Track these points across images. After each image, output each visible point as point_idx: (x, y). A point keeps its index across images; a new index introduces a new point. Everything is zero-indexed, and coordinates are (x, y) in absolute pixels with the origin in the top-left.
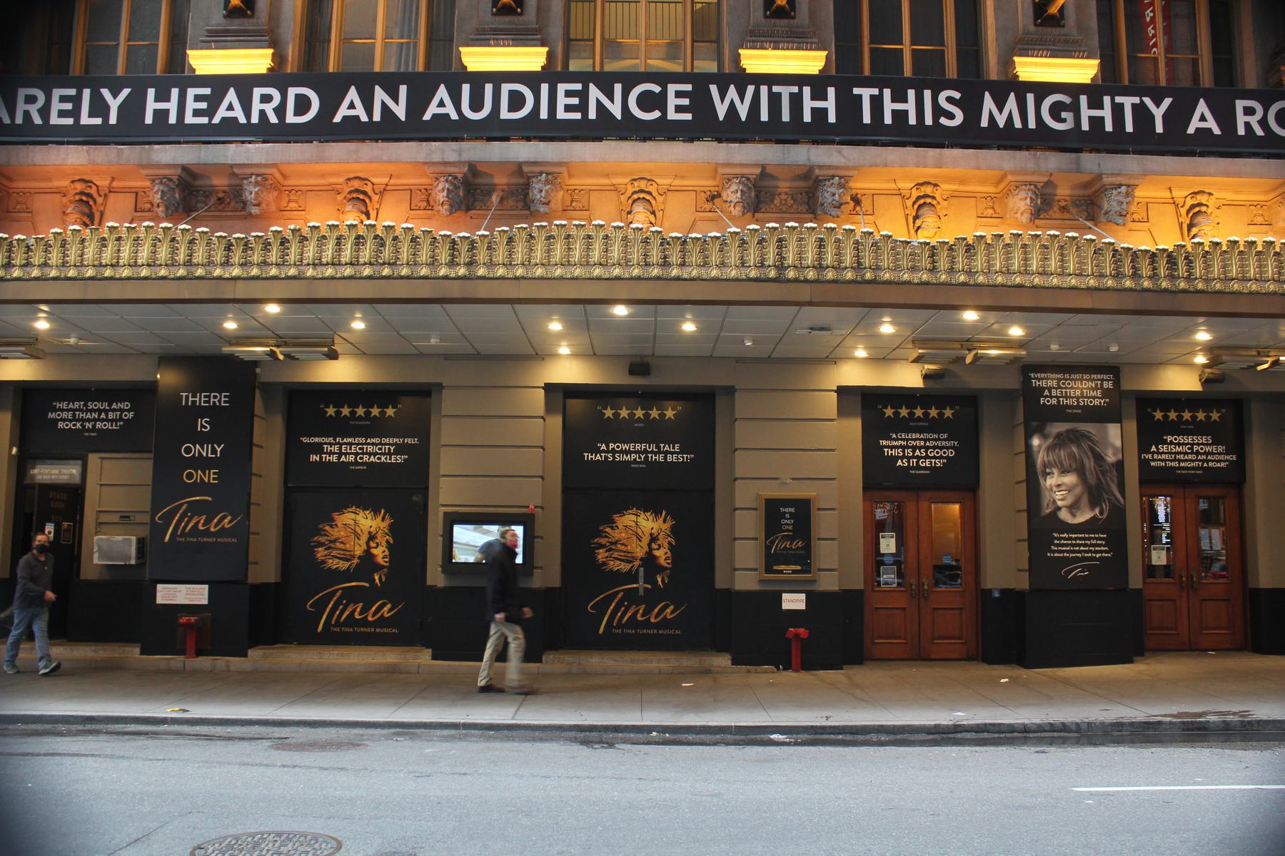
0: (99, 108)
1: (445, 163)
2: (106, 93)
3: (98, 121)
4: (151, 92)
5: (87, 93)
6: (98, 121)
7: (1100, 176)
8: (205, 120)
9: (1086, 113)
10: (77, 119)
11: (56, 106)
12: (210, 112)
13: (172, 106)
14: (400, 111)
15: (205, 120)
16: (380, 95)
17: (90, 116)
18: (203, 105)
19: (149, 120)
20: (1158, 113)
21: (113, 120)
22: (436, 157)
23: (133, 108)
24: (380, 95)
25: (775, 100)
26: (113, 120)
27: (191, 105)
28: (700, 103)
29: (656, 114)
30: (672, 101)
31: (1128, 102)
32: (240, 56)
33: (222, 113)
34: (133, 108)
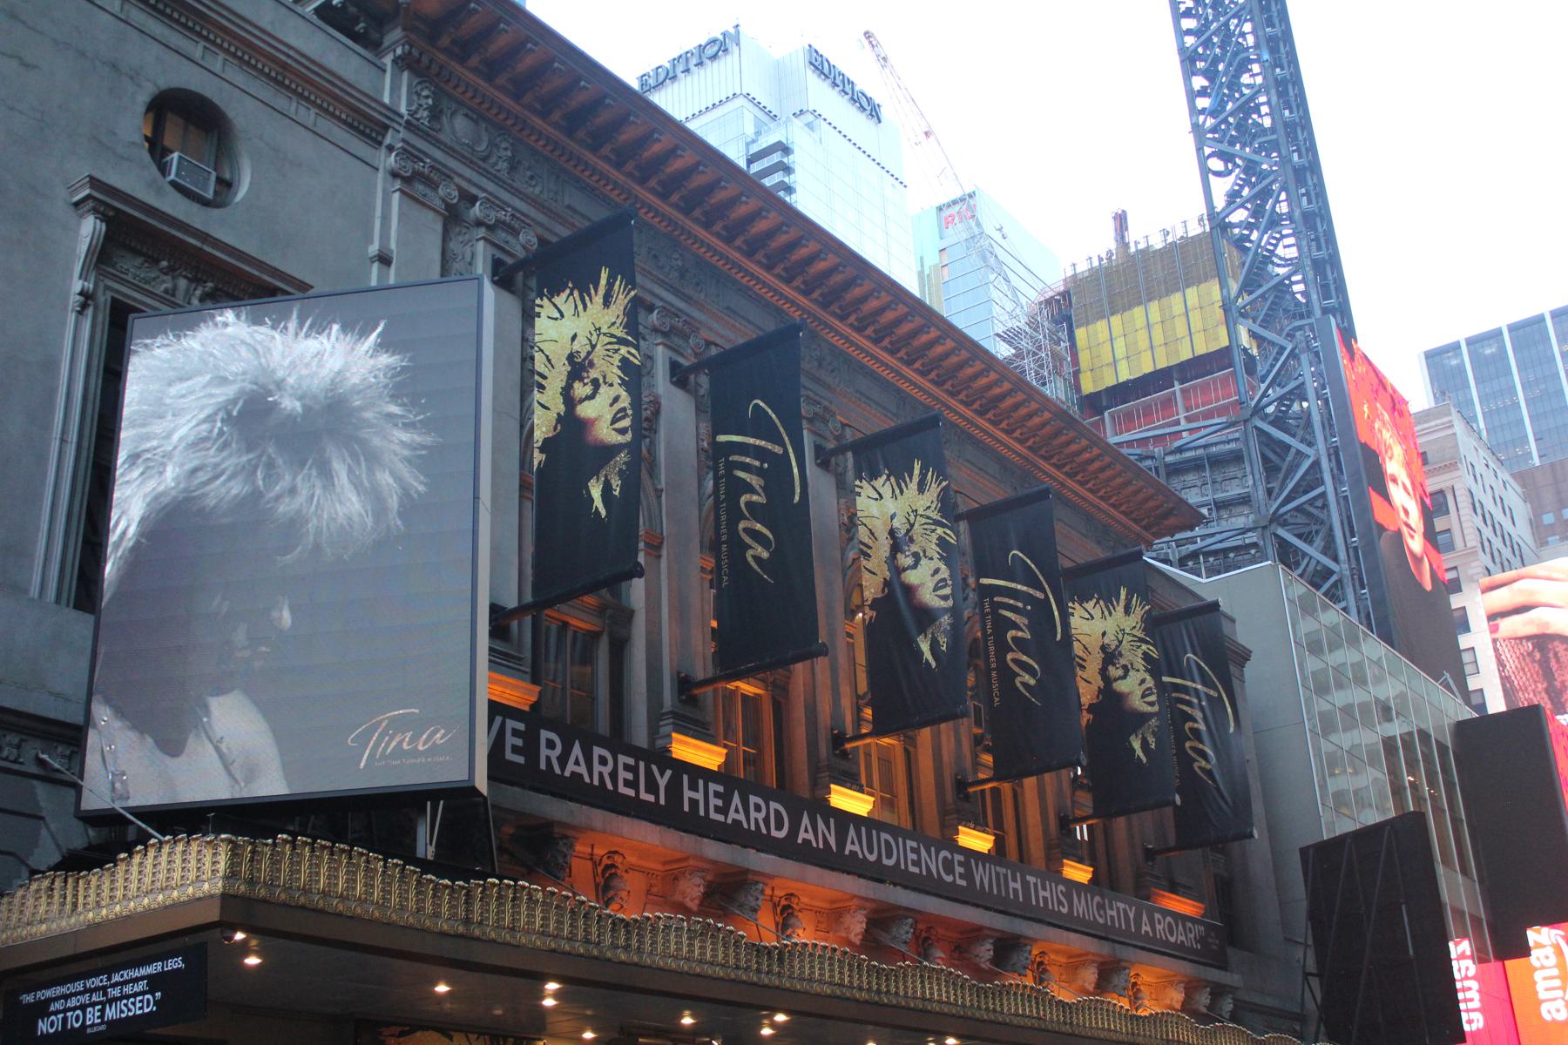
0: (652, 787)
1: (866, 899)
2: (654, 767)
3: (651, 798)
4: (685, 778)
5: (642, 764)
6: (651, 798)
7: (1120, 961)
8: (721, 818)
9: (1109, 912)
10: (638, 793)
11: (623, 774)
12: (723, 810)
13: (699, 796)
14: (832, 841)
15: (721, 818)
16: (821, 825)
17: (647, 791)
18: (720, 803)
19: (686, 808)
20: (1131, 916)
21: (662, 802)
22: (863, 893)
23: (674, 789)
24: (821, 825)
25: (998, 874)
26: (662, 802)
27: (714, 801)
28: (968, 875)
29: (949, 879)
30: (959, 870)
31: (1121, 906)
32: (709, 751)
33: (732, 815)
34: (674, 789)
